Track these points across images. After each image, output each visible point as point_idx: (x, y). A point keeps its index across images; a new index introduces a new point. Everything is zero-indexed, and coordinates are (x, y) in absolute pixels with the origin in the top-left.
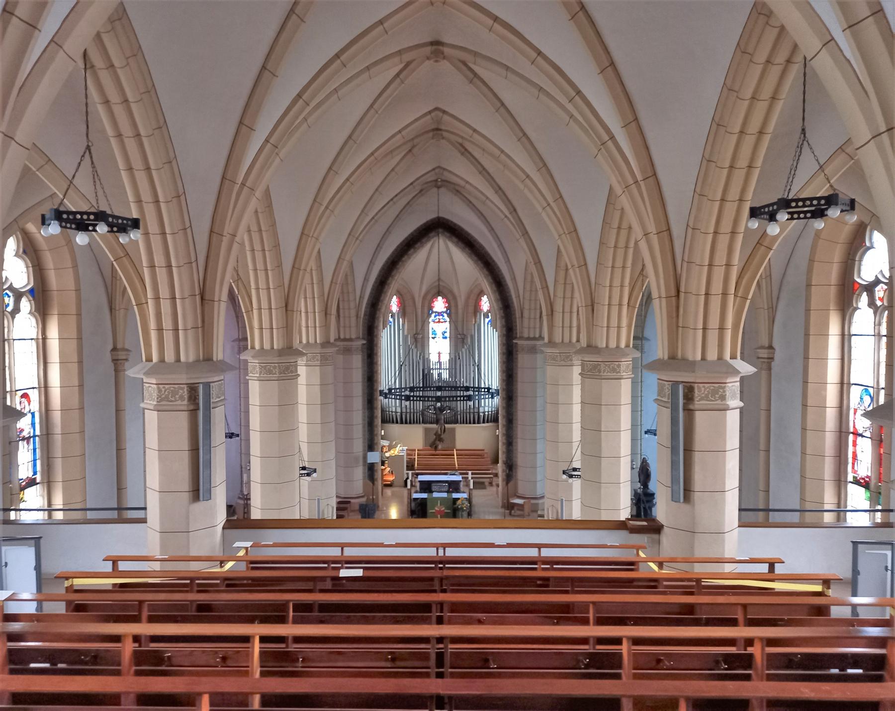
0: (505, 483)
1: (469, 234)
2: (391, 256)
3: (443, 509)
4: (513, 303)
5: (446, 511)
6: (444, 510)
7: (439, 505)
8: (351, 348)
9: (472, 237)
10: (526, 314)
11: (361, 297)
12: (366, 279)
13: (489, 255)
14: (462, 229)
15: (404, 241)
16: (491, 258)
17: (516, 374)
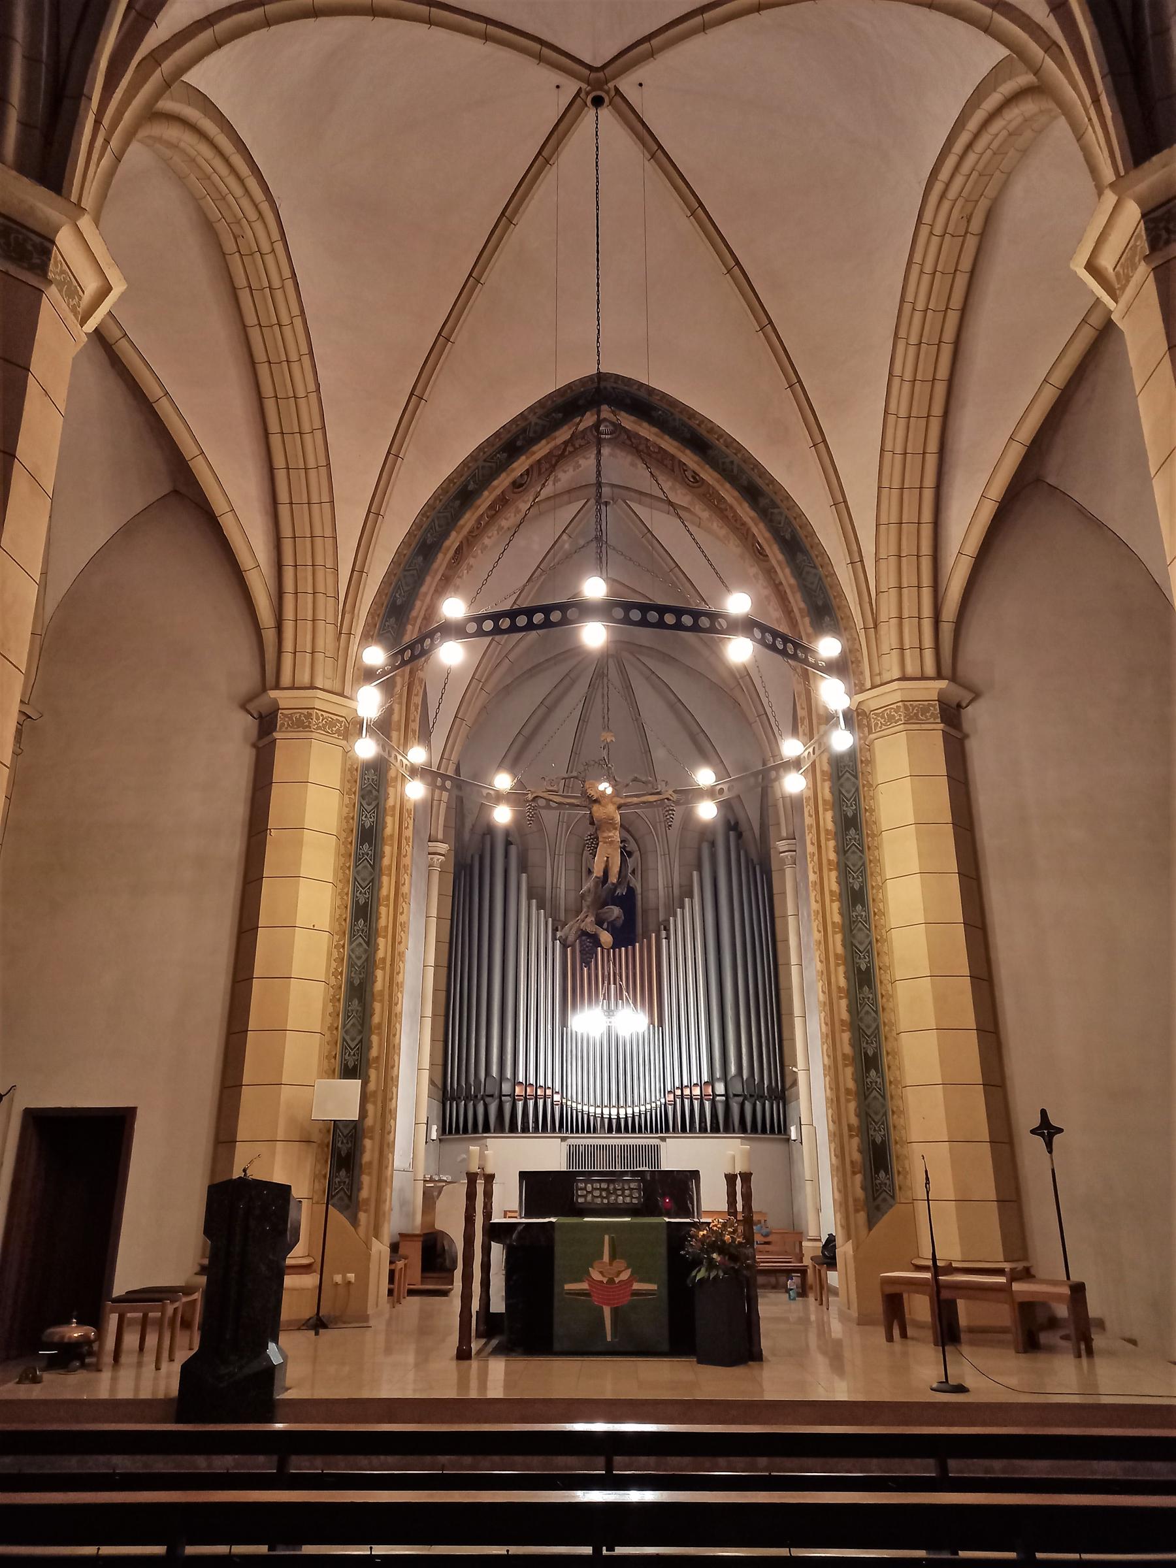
0: (862, 1217)
1: (693, 414)
2: (458, 472)
3: (625, 1276)
4: (841, 595)
5: (636, 1286)
6: (629, 1282)
7: (606, 1258)
8: (309, 716)
9: (704, 420)
10: (887, 608)
11: (358, 571)
12: (374, 513)
13: (757, 465)
14: (674, 403)
15: (497, 435)
16: (763, 473)
17: (872, 811)
